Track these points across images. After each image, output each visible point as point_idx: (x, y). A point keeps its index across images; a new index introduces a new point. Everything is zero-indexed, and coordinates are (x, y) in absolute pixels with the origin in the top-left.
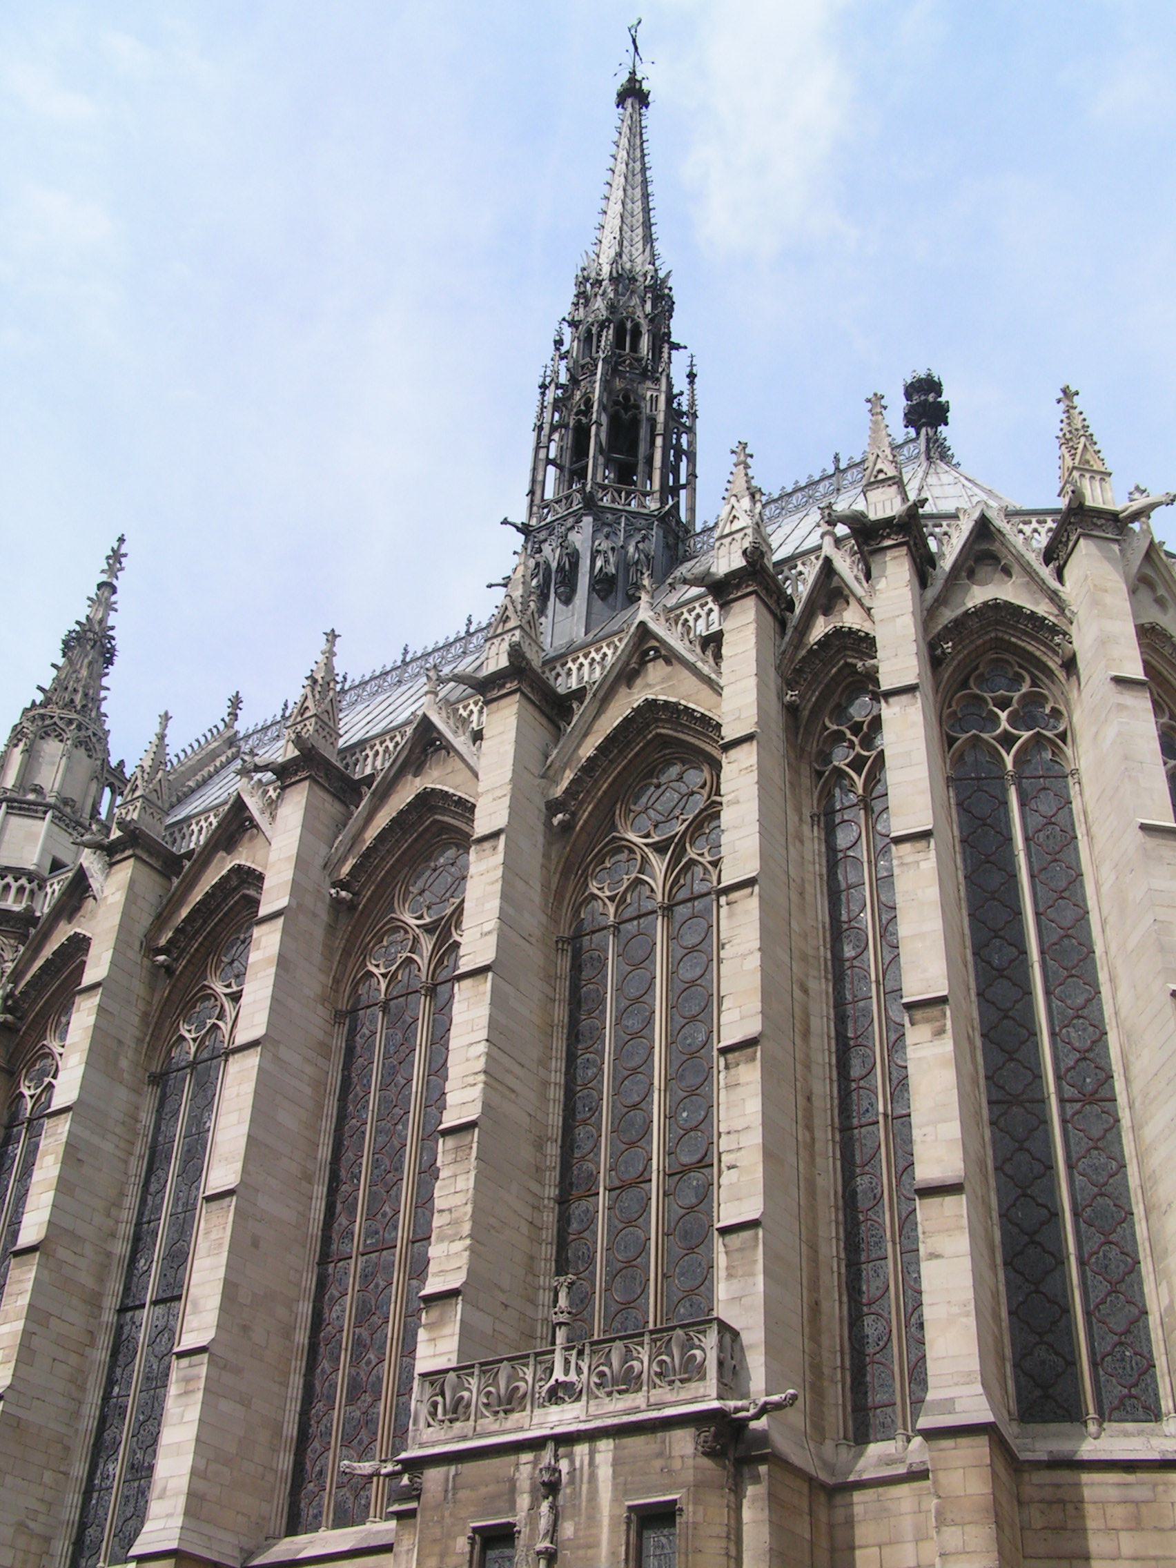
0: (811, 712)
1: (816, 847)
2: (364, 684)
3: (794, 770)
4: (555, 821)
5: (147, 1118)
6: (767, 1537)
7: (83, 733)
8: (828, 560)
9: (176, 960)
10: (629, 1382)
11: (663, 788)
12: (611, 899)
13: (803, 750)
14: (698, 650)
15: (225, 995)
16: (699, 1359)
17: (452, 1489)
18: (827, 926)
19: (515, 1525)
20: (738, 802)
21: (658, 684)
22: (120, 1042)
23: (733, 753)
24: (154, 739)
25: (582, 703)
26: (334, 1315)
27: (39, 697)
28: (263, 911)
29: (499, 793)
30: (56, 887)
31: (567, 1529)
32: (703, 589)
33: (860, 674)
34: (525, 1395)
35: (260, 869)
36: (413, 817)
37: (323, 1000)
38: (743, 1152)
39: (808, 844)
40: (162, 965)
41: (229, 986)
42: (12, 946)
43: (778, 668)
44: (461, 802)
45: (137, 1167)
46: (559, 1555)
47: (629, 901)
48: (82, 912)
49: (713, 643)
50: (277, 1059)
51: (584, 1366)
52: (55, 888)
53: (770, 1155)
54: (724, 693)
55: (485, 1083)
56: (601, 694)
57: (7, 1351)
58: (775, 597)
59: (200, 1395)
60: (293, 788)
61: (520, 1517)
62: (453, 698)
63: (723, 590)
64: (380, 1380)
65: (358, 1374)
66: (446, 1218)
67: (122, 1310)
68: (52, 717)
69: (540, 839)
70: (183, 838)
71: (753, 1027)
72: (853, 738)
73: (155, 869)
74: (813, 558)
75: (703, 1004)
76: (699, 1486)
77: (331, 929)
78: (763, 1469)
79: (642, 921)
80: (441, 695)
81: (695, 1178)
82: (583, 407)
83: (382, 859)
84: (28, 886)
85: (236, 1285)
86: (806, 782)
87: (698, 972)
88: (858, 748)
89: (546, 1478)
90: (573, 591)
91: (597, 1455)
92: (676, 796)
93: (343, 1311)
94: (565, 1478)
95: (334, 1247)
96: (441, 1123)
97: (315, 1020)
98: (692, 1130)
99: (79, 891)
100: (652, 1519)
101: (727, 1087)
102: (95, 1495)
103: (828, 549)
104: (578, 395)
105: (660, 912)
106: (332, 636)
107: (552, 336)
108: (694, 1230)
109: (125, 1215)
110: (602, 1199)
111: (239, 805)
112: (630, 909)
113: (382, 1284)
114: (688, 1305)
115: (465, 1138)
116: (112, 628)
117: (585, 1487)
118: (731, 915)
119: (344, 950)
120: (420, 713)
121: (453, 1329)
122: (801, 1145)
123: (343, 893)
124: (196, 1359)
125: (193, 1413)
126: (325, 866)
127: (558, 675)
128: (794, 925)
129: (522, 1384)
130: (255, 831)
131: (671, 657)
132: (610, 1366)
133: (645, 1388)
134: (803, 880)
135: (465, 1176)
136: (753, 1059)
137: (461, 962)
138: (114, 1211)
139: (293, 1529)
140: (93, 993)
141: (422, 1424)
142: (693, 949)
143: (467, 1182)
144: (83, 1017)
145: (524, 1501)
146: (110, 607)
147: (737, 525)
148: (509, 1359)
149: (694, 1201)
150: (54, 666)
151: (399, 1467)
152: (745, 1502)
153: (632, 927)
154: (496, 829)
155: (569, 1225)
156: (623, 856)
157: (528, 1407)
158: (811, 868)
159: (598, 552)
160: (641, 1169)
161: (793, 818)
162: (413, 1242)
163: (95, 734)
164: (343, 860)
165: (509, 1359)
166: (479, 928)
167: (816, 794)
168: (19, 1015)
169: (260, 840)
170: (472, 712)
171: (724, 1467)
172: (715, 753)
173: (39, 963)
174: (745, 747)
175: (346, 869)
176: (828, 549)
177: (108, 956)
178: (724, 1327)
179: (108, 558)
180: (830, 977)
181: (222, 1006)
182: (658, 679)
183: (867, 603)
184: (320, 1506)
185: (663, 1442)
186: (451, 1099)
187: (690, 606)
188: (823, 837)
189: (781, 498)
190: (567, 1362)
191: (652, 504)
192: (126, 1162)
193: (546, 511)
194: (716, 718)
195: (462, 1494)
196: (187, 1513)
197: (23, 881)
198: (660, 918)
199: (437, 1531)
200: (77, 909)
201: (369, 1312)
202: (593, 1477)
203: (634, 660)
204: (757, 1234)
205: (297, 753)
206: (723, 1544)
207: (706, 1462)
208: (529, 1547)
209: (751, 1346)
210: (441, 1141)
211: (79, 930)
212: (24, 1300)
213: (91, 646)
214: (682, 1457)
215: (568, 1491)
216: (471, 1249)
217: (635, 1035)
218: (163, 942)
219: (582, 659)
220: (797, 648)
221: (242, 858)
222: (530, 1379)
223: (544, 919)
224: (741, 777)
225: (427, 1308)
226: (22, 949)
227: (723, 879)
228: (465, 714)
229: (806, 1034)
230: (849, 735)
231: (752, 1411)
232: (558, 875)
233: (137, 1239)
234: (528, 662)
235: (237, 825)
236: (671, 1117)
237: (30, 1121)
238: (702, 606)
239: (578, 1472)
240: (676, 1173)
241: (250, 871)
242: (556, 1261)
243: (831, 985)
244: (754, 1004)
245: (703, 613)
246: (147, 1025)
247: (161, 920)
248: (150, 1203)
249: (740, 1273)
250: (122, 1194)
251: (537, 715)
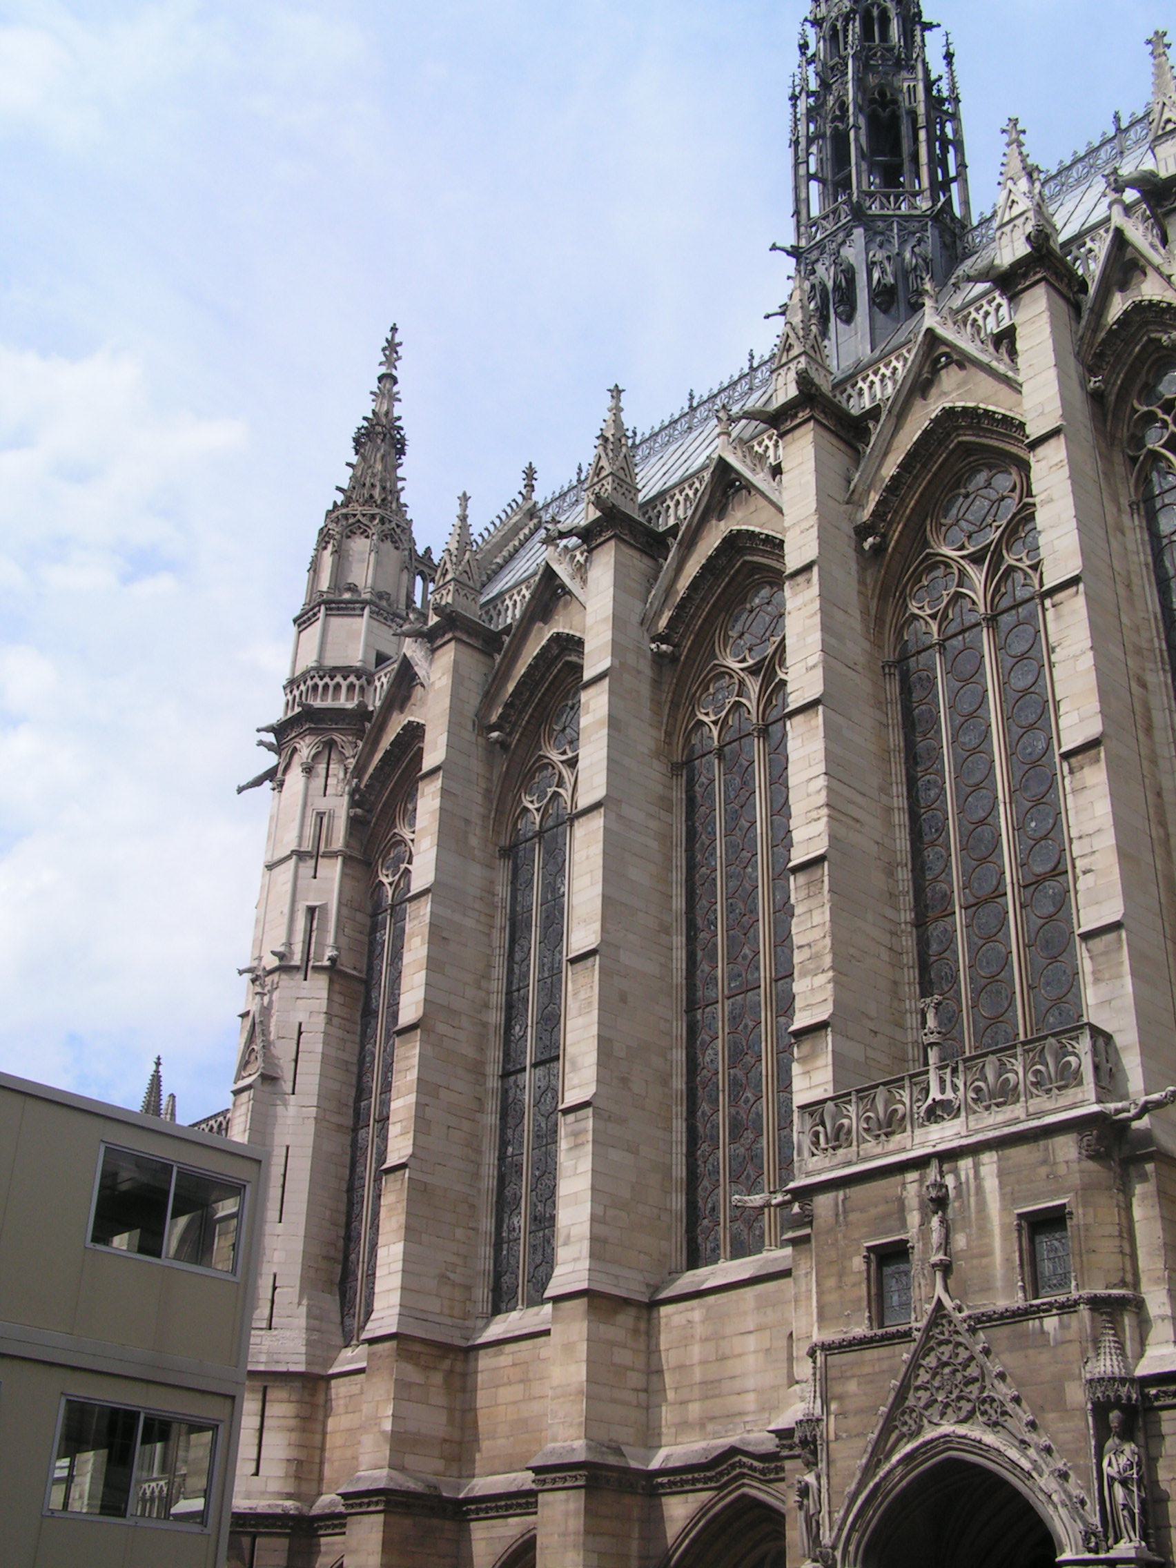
0: (1118, 395)
1: (1139, 536)
2: (654, 435)
3: (1107, 459)
4: (866, 546)
5: (503, 891)
6: (1160, 1233)
7: (387, 526)
8: (1119, 232)
9: (510, 734)
10: (1006, 1094)
11: (972, 497)
12: (933, 617)
13: (1113, 437)
14: (991, 349)
15: (562, 762)
16: (1074, 1065)
17: (842, 1213)
18: (1159, 616)
19: (907, 1241)
20: (1052, 500)
21: (953, 391)
22: (467, 822)
23: (1041, 451)
24: (456, 521)
25: (878, 422)
26: (708, 1059)
27: (340, 498)
28: (587, 675)
29: (805, 525)
30: (384, 680)
31: (960, 1241)
32: (988, 285)
33: (1166, 348)
34: (904, 1117)
35: (578, 634)
36: (723, 561)
37: (658, 754)
38: (1097, 855)
39: (1129, 533)
40: (497, 741)
41: (564, 753)
42: (351, 743)
43: (1077, 355)
44: (769, 539)
45: (500, 939)
46: (954, 1266)
47: (951, 616)
48: (412, 701)
49: (1006, 339)
50: (620, 816)
51: (960, 1083)
52: (383, 681)
53: (1125, 854)
54: (1024, 390)
55: (829, 816)
56: (895, 412)
57: (404, 1123)
58: (1066, 280)
59: (589, 1147)
60: (599, 549)
61: (912, 1232)
62: (746, 436)
63: (1009, 282)
64: (759, 1116)
65: (738, 1113)
66: (806, 953)
67: (505, 1075)
68: (355, 515)
69: (854, 566)
70: (499, 614)
71: (1094, 728)
72: (1166, 417)
73: (475, 648)
74: (1102, 232)
75: (1039, 712)
76: (1086, 1190)
77: (656, 683)
78: (1149, 1167)
79: (967, 635)
80: (734, 435)
81: (1051, 887)
82: (838, 113)
83: (698, 607)
84: (357, 683)
85: (610, 1040)
86: (1120, 468)
87: (1030, 679)
88: (1172, 427)
89: (933, 1194)
90: (853, 308)
91: (982, 1168)
92: (986, 503)
93: (717, 1054)
94: (952, 1193)
95: (700, 994)
96: (790, 860)
97: (653, 775)
98: (1042, 839)
99: (406, 681)
100: (1042, 1225)
101: (1074, 791)
102: (505, 1246)
103: (1118, 219)
104: (831, 100)
105: (984, 624)
106: (616, 392)
107: (796, 41)
108: (1054, 939)
109: (494, 986)
110: (959, 918)
111: (549, 574)
112: (953, 625)
113: (751, 1024)
114: (1057, 1013)
115: (816, 873)
116: (399, 418)
117: (972, 1200)
118: (1058, 617)
119: (672, 702)
120: (715, 456)
121: (825, 1061)
122: (1156, 842)
123: (664, 647)
124: (581, 1114)
125: (586, 1165)
126: (642, 623)
127: (850, 396)
128: (1125, 619)
129: (899, 1106)
130: (568, 597)
131: (963, 361)
132: (985, 1080)
133: (1022, 1099)
134: (1129, 572)
135: (820, 910)
136: (1098, 760)
137: (790, 699)
138: (484, 984)
139: (694, 1261)
140: (434, 777)
141: (806, 1154)
142: (1022, 657)
143: (822, 916)
144: (428, 801)
145: (914, 1218)
146: (394, 398)
147: (1016, 210)
148: (884, 1084)
149: (1052, 909)
150: (348, 464)
151: (788, 1197)
152: (1135, 1201)
153: (957, 642)
154: (808, 561)
155: (929, 948)
156: (940, 572)
157: (909, 1128)
158: (1135, 558)
159: (874, 263)
160: (995, 883)
161: (1110, 508)
162: (776, 981)
163: (398, 526)
164: (659, 614)
165: (884, 1084)
166: (803, 663)
167: (1132, 481)
168: (367, 807)
169: (574, 606)
170: (767, 447)
171: (1110, 1169)
172: (1022, 453)
173: (379, 756)
174: (1053, 442)
175: (663, 622)
176: (1118, 219)
177: (443, 739)
178: (1096, 1032)
179: (384, 349)
180: (1167, 667)
181: (560, 773)
182: (954, 386)
183: (1166, 270)
184: (716, 1239)
185: (1046, 1149)
186: (797, 836)
187: (978, 305)
188: (1144, 524)
189: (1059, 173)
190: (942, 1081)
191: (924, 204)
192: (489, 935)
193: (814, 229)
194: (1018, 417)
195: (852, 1217)
196: (593, 1255)
197: (352, 679)
198: (985, 630)
199: (833, 1254)
200: (407, 698)
201: (741, 1053)
202: (979, 1189)
204: (1120, 936)
205: (598, 514)
206: (1117, 1242)
207: (1091, 1165)
208: (924, 1260)
209: (1126, 1048)
210: (792, 878)
211: (412, 719)
212: (413, 1075)
213: (381, 439)
214: (1067, 1162)
215: (956, 1204)
216: (835, 980)
217: (974, 751)
218: (494, 718)
219: (872, 377)
220: (1095, 331)
221: (559, 626)
222: (907, 1100)
223: (867, 645)
224: (1051, 474)
225: (798, 1043)
226: (360, 744)
227: (1045, 581)
228: (761, 451)
229: (1149, 730)
230: (1161, 415)
231: (1133, 1111)
232: (876, 600)
233: (510, 1007)
234: (818, 388)
235: (550, 593)
236: (1019, 827)
237: (393, 907)
238: (989, 302)
239: (964, 1186)
240: (1031, 885)
241: (570, 638)
242: (920, 984)
243: (1169, 675)
244: (1093, 704)
245: (992, 310)
246: (491, 802)
247: (489, 698)
248: (517, 971)
249: (1107, 976)
250: (490, 966)
251: (834, 441)
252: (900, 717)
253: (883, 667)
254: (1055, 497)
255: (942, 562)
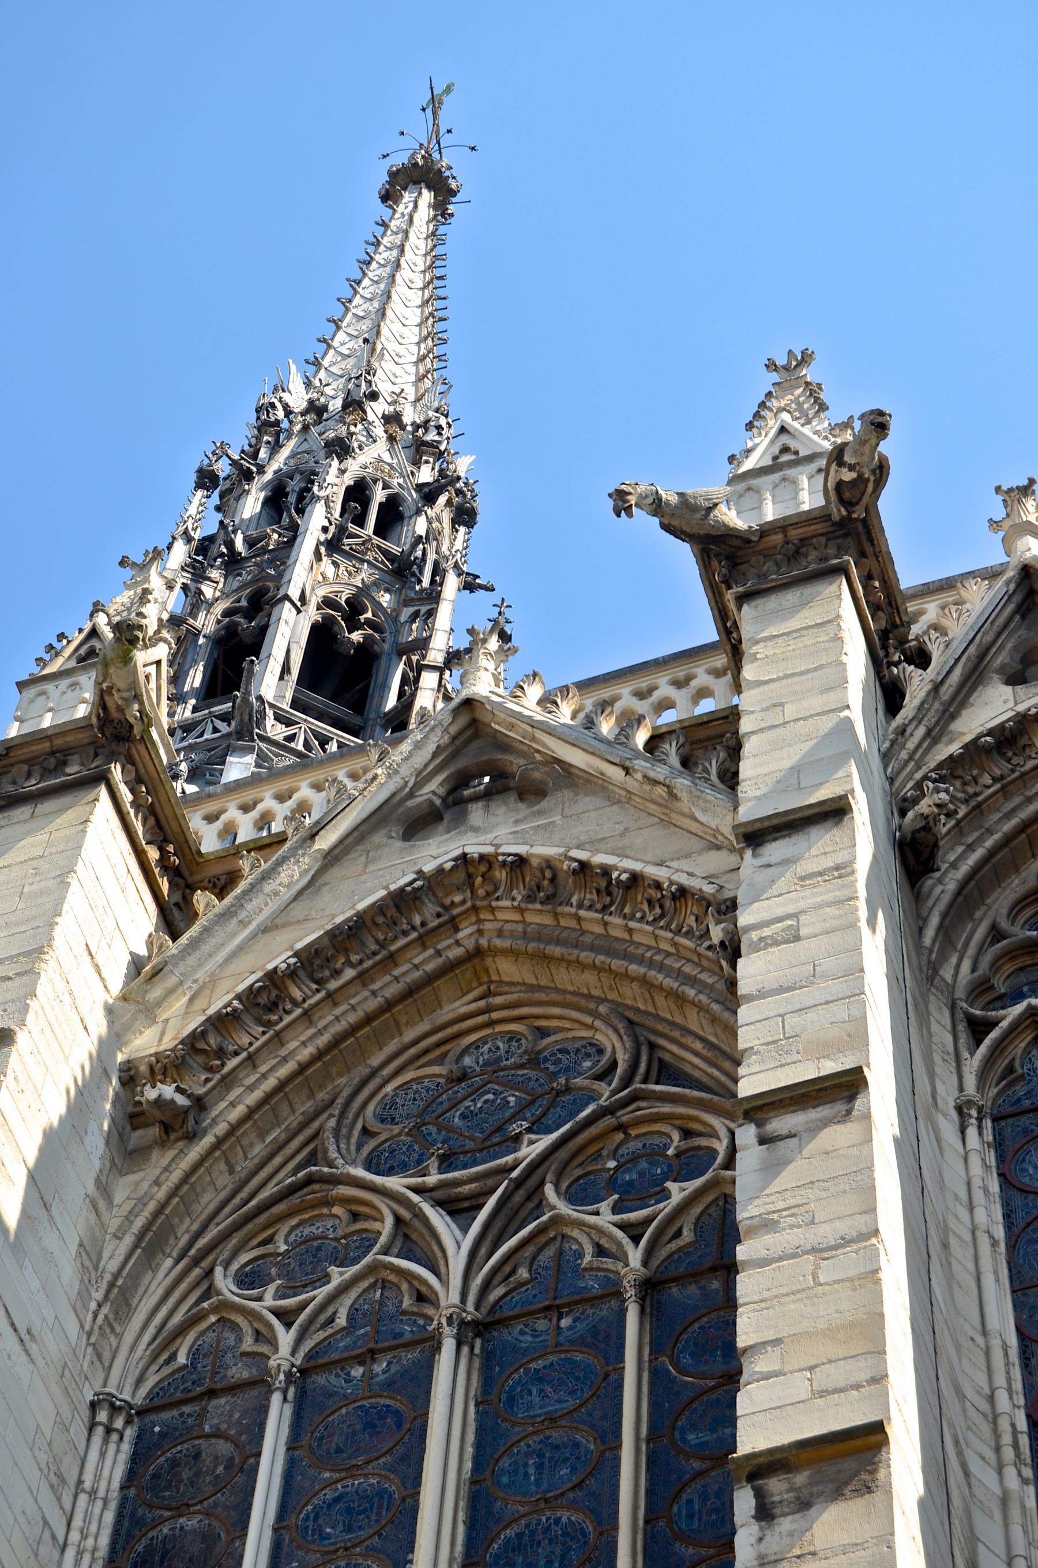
12: (286, 1317)
20: (797, 938)
167: (973, 1063)
203: (435, 785)
220: (934, 736)
232: (129, 1240)
252: (104, 1541)
253: (93, 1406)
254: (803, 932)
255: (344, 1201)
